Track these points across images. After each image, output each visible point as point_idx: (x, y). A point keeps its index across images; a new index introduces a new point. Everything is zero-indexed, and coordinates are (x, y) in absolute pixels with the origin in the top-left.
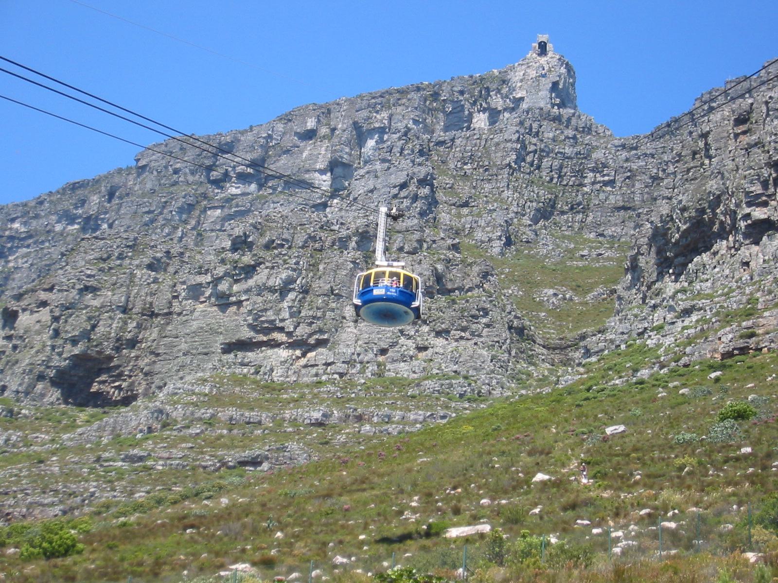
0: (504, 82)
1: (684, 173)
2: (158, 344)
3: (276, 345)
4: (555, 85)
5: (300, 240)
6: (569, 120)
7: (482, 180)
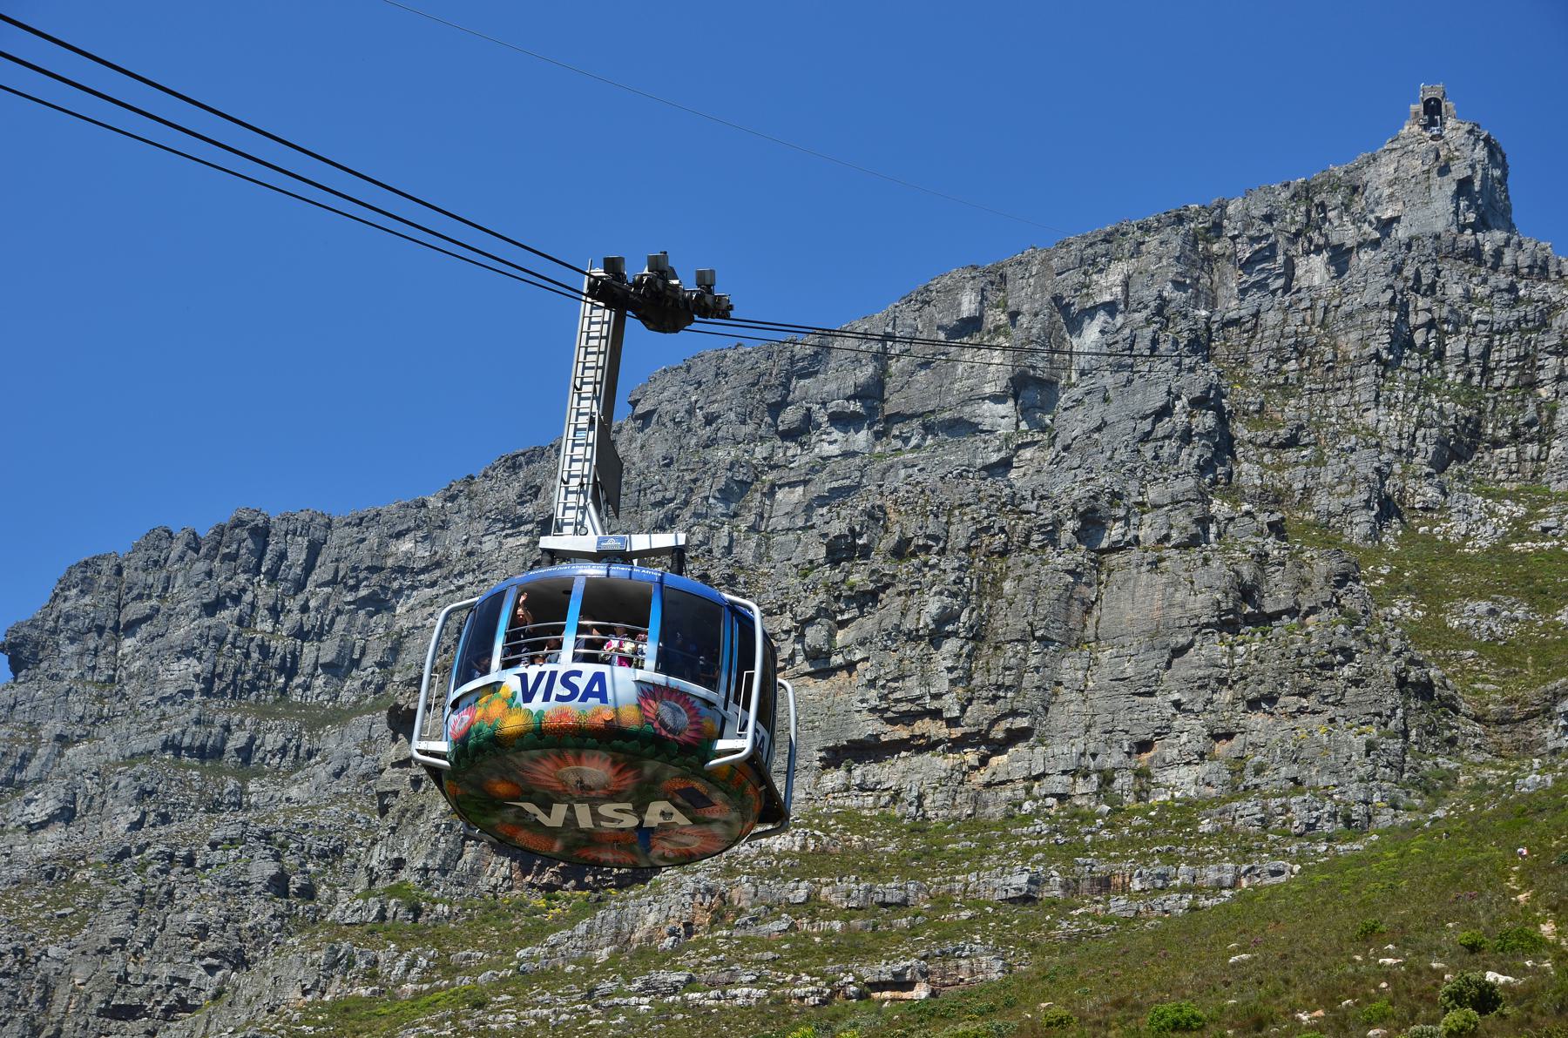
0: (1355, 189)
3: (931, 746)
4: (1464, 186)
5: (960, 533)
6: (1498, 254)
7: (1323, 391)
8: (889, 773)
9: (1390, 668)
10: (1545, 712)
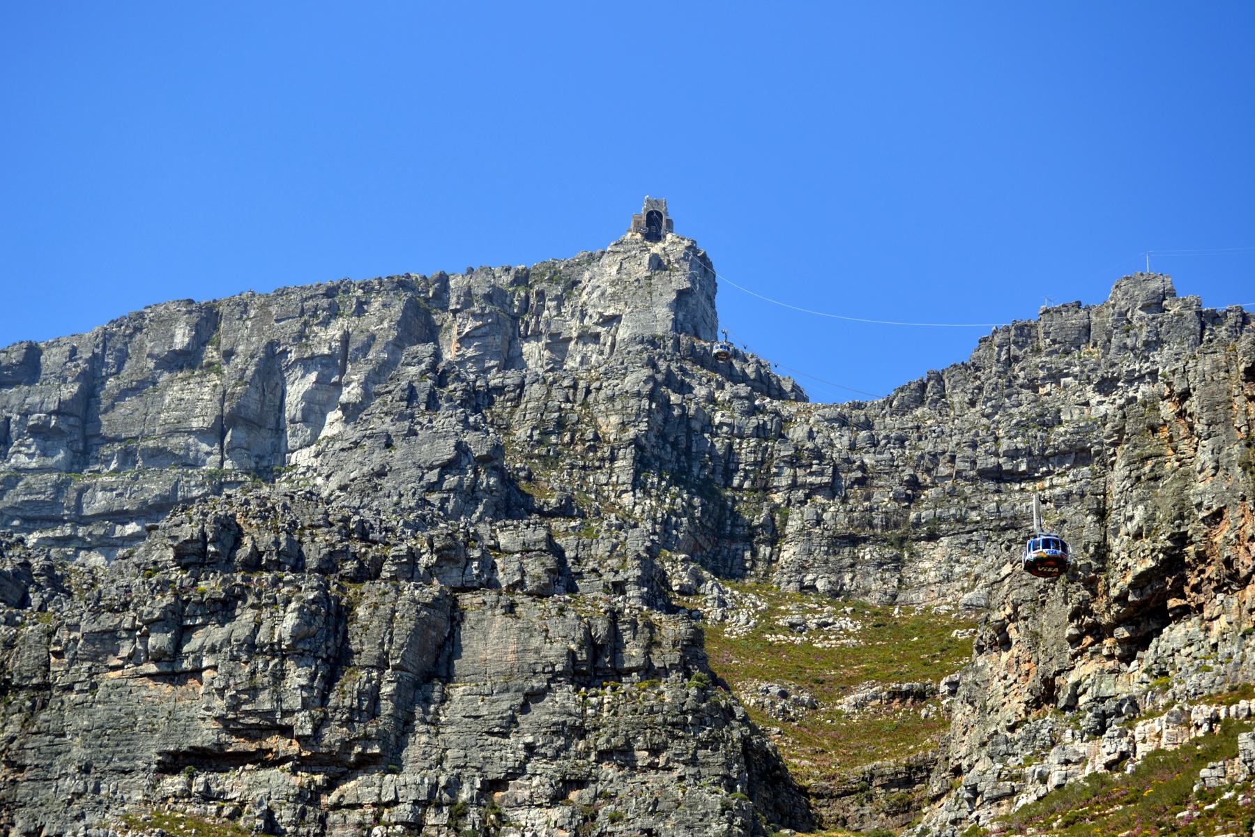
1: (1133, 467)
2: (21, 747)
5: (313, 553)
7: (584, 468)
8: (235, 783)
9: (736, 734)
10: (862, 791)
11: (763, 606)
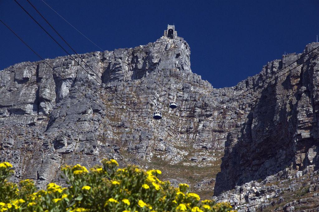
11: (187, 154)
